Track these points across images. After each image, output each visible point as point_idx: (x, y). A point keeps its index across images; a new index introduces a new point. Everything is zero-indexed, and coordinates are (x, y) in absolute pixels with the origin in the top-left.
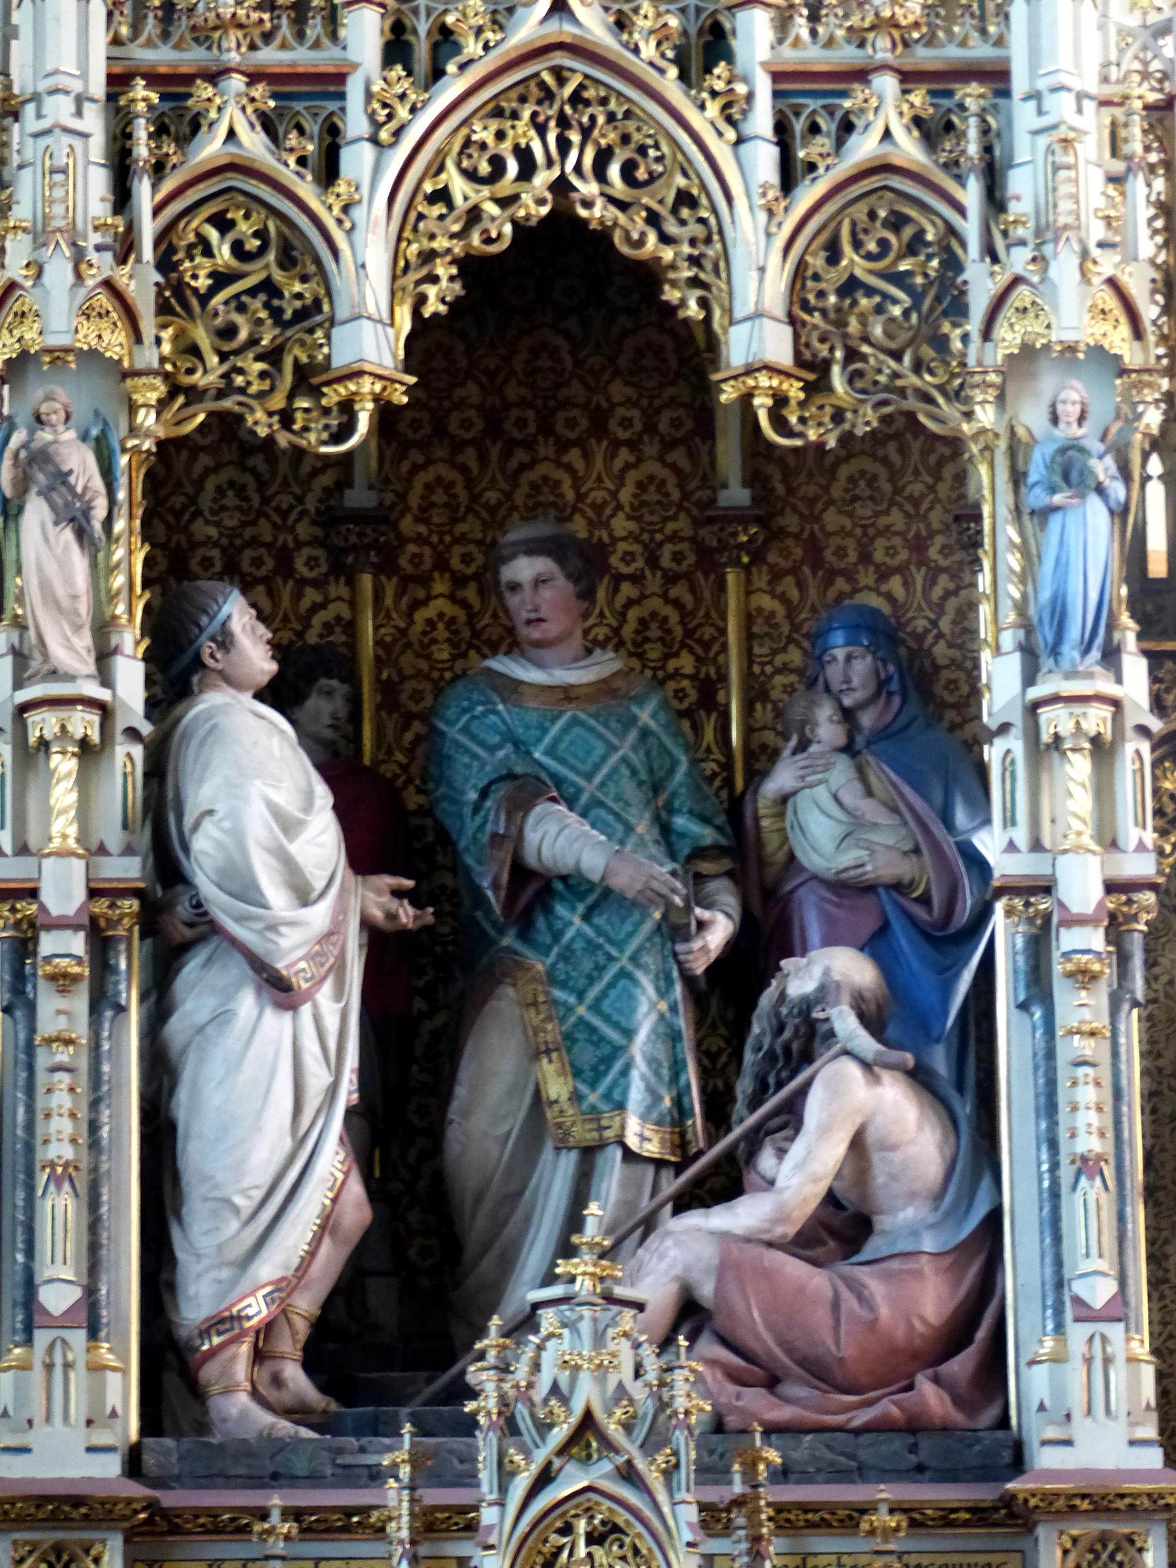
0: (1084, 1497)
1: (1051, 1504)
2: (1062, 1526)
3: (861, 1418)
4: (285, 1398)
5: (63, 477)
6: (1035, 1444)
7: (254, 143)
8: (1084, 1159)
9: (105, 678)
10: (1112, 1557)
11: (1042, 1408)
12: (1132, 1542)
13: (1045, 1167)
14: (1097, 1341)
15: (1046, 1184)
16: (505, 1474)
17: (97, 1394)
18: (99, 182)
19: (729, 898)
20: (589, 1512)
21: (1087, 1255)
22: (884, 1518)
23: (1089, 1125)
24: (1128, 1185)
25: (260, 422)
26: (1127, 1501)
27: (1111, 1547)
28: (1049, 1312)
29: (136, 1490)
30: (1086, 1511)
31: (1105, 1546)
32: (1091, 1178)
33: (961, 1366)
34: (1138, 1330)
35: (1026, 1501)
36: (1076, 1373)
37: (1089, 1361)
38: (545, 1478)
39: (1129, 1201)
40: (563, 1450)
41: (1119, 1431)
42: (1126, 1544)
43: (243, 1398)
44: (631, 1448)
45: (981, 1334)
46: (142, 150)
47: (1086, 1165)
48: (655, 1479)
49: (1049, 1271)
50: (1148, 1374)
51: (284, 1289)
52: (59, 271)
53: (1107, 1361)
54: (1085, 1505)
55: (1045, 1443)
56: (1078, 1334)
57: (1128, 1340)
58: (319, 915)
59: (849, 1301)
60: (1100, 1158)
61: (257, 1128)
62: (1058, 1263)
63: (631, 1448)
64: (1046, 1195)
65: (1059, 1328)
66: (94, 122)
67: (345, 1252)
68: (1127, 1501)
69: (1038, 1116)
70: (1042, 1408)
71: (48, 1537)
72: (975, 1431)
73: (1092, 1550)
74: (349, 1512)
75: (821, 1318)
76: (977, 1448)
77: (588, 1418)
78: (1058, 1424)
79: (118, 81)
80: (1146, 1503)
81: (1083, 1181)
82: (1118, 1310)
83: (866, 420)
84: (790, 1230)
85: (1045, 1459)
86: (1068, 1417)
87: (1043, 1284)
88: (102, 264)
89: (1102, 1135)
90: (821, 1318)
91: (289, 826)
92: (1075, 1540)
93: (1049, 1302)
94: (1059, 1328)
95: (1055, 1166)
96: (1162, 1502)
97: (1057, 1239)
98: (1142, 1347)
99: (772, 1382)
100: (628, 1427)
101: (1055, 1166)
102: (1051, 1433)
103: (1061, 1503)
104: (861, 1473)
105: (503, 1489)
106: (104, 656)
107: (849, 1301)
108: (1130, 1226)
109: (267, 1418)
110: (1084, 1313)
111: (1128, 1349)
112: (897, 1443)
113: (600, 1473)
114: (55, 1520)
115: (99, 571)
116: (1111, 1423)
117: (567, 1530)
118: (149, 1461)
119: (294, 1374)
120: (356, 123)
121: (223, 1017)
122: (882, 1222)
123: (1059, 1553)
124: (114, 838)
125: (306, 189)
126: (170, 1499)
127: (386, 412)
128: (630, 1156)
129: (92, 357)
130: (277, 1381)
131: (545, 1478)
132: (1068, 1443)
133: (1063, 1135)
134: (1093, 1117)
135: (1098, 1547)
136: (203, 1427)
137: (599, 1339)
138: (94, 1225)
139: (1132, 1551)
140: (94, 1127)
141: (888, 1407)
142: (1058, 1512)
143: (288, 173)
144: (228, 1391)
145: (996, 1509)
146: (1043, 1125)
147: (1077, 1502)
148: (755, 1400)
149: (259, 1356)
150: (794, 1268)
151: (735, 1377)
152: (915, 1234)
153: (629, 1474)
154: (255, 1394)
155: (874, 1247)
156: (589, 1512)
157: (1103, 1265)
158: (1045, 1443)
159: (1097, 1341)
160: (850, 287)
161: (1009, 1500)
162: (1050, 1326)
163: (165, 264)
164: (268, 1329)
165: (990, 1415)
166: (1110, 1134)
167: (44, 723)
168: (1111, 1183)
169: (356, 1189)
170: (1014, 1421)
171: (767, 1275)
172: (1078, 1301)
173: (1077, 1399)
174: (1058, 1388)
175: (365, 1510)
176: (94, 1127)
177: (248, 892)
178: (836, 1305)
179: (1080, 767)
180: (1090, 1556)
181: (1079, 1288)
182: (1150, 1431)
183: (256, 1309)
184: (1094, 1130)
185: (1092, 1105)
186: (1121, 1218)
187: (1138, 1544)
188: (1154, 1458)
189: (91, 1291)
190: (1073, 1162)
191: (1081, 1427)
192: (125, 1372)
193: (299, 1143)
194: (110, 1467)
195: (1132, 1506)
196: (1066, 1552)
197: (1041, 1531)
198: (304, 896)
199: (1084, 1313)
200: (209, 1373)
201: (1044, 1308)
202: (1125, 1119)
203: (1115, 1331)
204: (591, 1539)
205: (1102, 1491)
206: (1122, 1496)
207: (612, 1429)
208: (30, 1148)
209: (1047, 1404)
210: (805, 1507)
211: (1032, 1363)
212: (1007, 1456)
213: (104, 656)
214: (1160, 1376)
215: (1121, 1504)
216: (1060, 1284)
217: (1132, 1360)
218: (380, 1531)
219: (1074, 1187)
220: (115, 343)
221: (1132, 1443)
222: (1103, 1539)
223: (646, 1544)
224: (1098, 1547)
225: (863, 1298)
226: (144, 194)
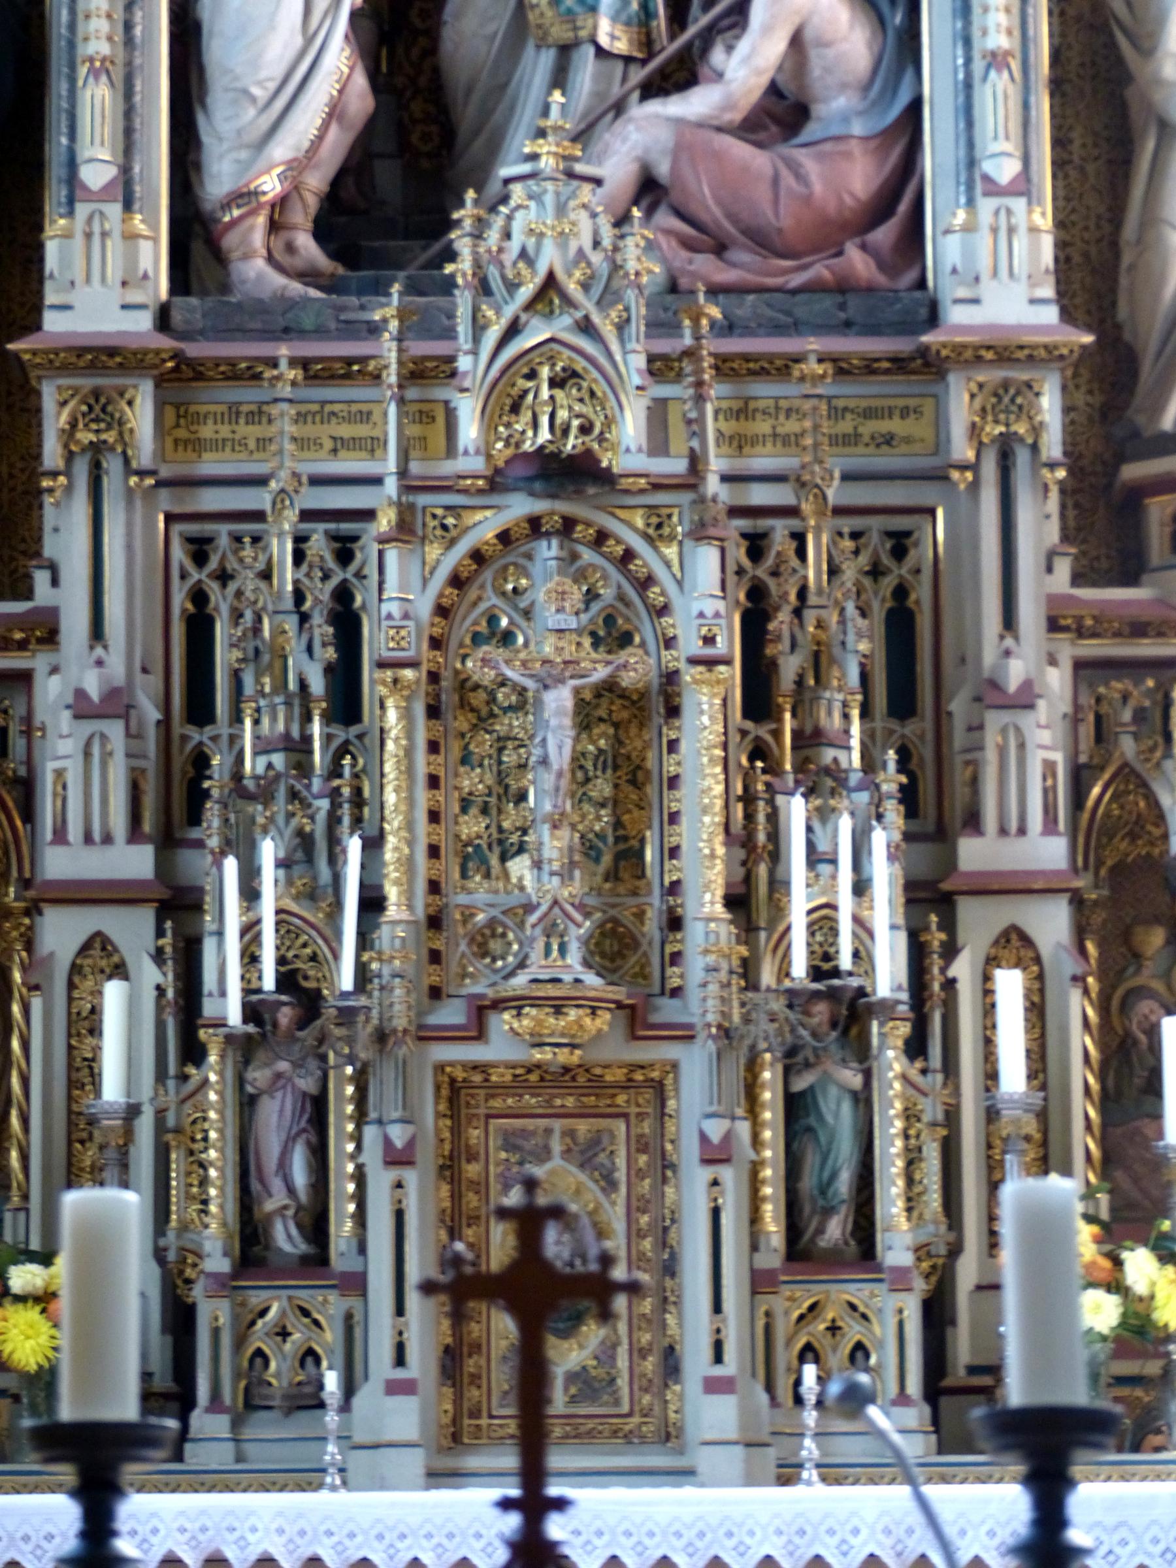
0: (989, 348)
1: (960, 354)
2: (971, 373)
3: (796, 280)
4: (298, 263)
6: (948, 303)
8: (994, 54)
10: (1013, 401)
11: (954, 271)
12: (1030, 387)
13: (960, 61)
14: (1003, 213)
15: (961, 76)
16: (479, 327)
17: (131, 259)
20: (552, 360)
21: (996, 138)
22: (813, 367)
23: (998, 25)
24: (1032, 76)
26: (1026, 352)
27: (1012, 391)
28: (962, 188)
29: (165, 342)
30: (991, 361)
31: (1006, 391)
32: (999, 71)
33: (884, 235)
34: (1040, 203)
35: (938, 352)
36: (984, 241)
37: (995, 230)
38: (513, 330)
39: (1033, 91)
40: (529, 306)
41: (1021, 290)
42: (1025, 389)
43: (259, 264)
44: (588, 305)
45: (903, 207)
47: (996, 60)
48: (608, 331)
49: (962, 153)
50: (1047, 245)
51: (296, 168)
53: (1011, 230)
54: (989, 355)
55: (957, 301)
56: (986, 206)
57: (1030, 212)
59: (788, 179)
60: (1008, 53)
61: (272, 27)
62: (970, 145)
63: (588, 305)
64: (960, 86)
65: (971, 202)
67: (349, 138)
68: (1026, 352)
69: (954, 17)
70: (954, 271)
71: (87, 383)
72: (896, 291)
73: (996, 395)
74: (349, 361)
75: (763, 194)
76: (898, 306)
77: (551, 280)
78: (968, 285)
80: (1043, 353)
81: (993, 74)
82: (1023, 186)
84: (737, 116)
85: (956, 315)
86: (977, 279)
87: (957, 164)
89: (1009, 32)
90: (763, 194)
92: (981, 386)
93: (963, 179)
94: (971, 202)
95: (968, 61)
96: (1056, 353)
97: (970, 124)
98: (1044, 218)
99: (720, 249)
100: (585, 286)
101: (968, 61)
102: (962, 293)
103: (968, 354)
104: (796, 327)
105: (476, 339)
107: (788, 179)
108: (1033, 113)
109: (278, 280)
110: (993, 189)
111: (1030, 220)
112: (827, 302)
113: (561, 325)
114: (93, 367)
116: (1013, 285)
117: (532, 375)
118: (177, 317)
119: (305, 242)
122: (819, 110)
123: (966, 397)
126: (194, 350)
128: (601, 52)
130: (290, 248)
131: (513, 330)
132: (976, 301)
133: (976, 33)
134: (1002, 18)
135: (1001, 391)
136: (225, 288)
137: (561, 210)
138: (129, 113)
139: (1030, 395)
140: (128, 26)
141: (820, 270)
142: (966, 361)
144: (247, 256)
145: (913, 359)
146: (959, 25)
147: (983, 353)
148: (705, 265)
149: (274, 227)
150: (740, 150)
151: (689, 245)
152: (846, 119)
153: (586, 327)
154: (270, 259)
155: (811, 131)
156: (552, 360)
157: (1008, 147)
158: (957, 301)
159: (1003, 213)
161: (923, 352)
162: (963, 200)
164: (282, 202)
165: (911, 276)
166: (1017, 33)
168: (1017, 75)
169: (360, 81)
170: (930, 283)
171: (718, 156)
172: (986, 178)
173: (984, 263)
174: (969, 253)
175: (363, 360)
176: (128, 26)
178: (776, 181)
180: (994, 400)
181: (987, 167)
182: (1048, 291)
183: (271, 185)
184: (1003, 29)
185: (1002, 8)
186: (1026, 106)
187: (1036, 389)
188: (1050, 315)
189: (126, 170)
190: (984, 57)
191: (987, 288)
192: (155, 240)
193: (309, 40)
194: (143, 322)
195: (1030, 357)
196: (973, 396)
197: (952, 378)
199: (993, 189)
200: (230, 241)
201: (958, 183)
202: (1031, 20)
203: (1019, 205)
204: (554, 383)
205: (1005, 343)
206: (1021, 347)
207: (572, 287)
208: (72, 45)
209: (959, 268)
210: (746, 358)
211: (947, 232)
212: (924, 312)
214: (1061, 246)
215: (1021, 355)
216: (972, 163)
217: (1033, 230)
218: (377, 377)
219: (985, 78)
221: (1033, 301)
222: (1006, 385)
223: (601, 388)
224: (1001, 391)
225: (799, 175)
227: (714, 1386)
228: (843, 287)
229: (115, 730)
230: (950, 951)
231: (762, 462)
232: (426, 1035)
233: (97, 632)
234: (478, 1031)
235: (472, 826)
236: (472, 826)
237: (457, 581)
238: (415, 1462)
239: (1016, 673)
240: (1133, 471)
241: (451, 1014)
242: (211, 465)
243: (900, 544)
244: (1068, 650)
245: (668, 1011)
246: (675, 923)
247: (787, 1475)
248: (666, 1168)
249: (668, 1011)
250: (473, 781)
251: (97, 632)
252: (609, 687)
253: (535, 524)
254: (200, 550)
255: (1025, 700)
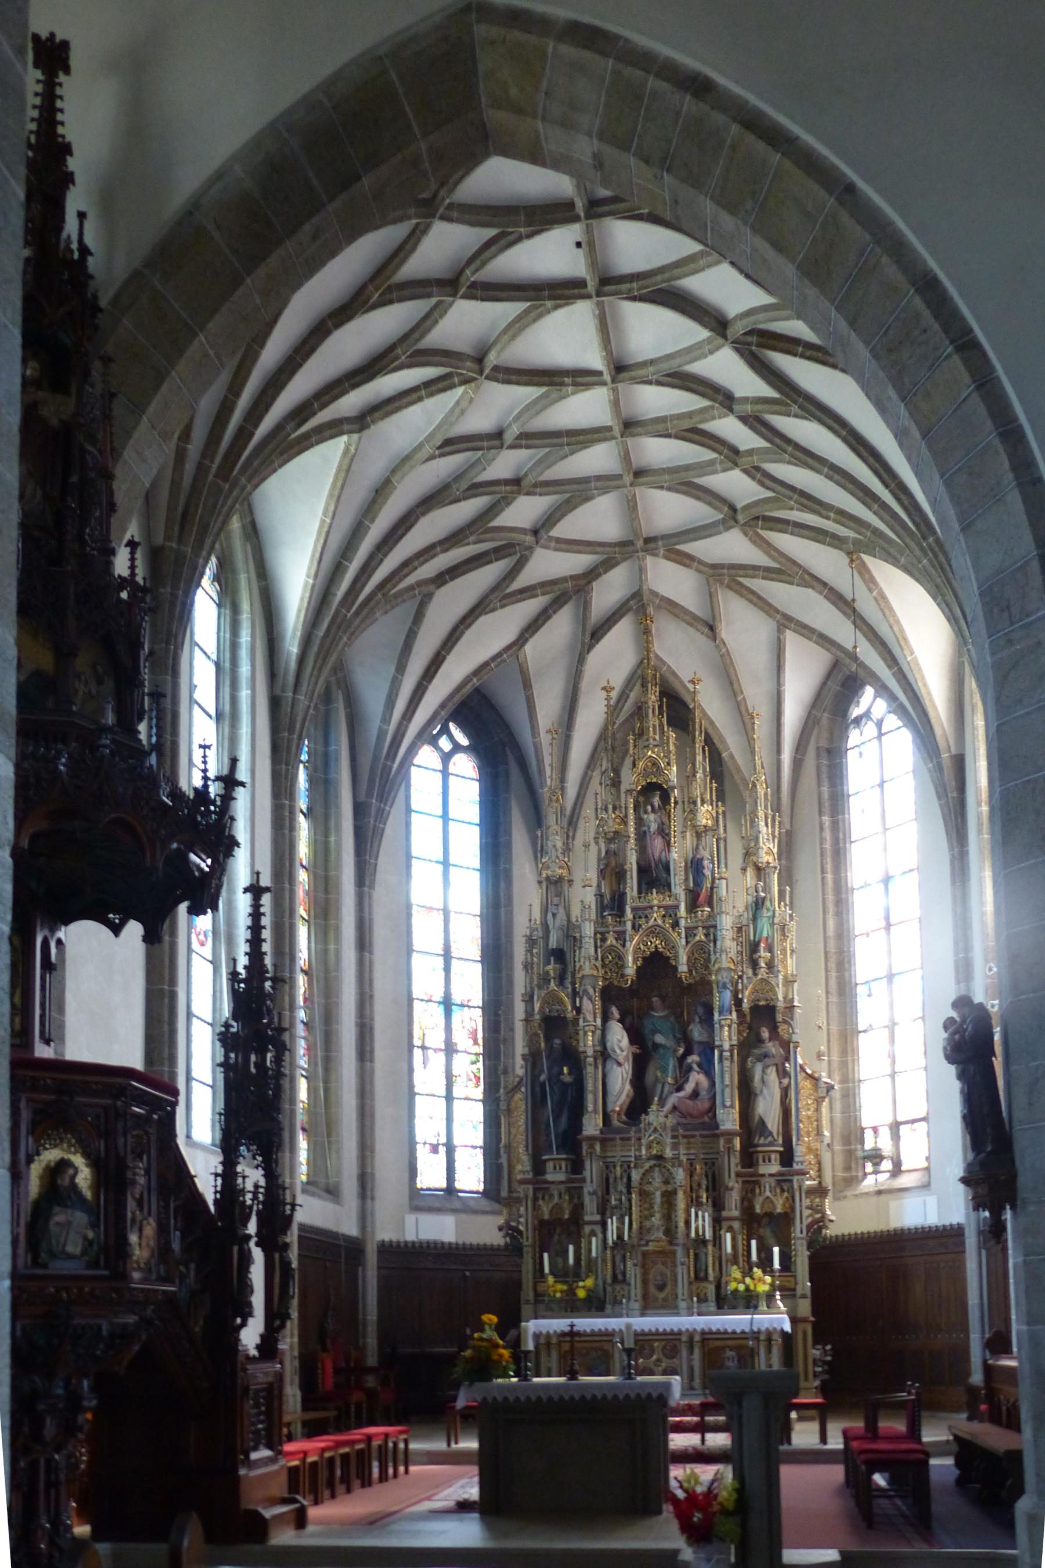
5: (588, 993)
7: (614, 942)
9: (595, 1021)
18: (593, 949)
19: (683, 1045)
25: (616, 983)
33: (710, 1114)
46: (599, 944)
51: (621, 1107)
52: (587, 963)
58: (625, 1053)
66: (592, 941)
79: (595, 934)
83: (697, 979)
85: (722, 1128)
88: (593, 962)
91: (620, 1041)
106: (595, 1017)
115: (594, 1005)
120: (628, 938)
121: (612, 1068)
124: (596, 1043)
125: (621, 948)
127: (632, 981)
129: (592, 975)
141: (700, 1121)
143: (618, 946)
148: (683, 1121)
160: (696, 959)
163: (602, 960)
167: (587, 1028)
177: (614, 1051)
179: (726, 1028)
183: (617, 1109)
198: (622, 1051)
213: (595, 1017)
220: (595, 973)
226: (599, 950)
227: (683, 1300)
228: (704, 1123)
229: (594, 1197)
230: (720, 1229)
231: (693, 1151)
232: (640, 1246)
233: (592, 1181)
234: (647, 1245)
235: (646, 1213)
236: (646, 1213)
237: (644, 1174)
238: (637, 1312)
239: (730, 1184)
240: (751, 1150)
241: (643, 1242)
242: (609, 1154)
243: (713, 1164)
244: (740, 1180)
245: (676, 1241)
246: (676, 1227)
247: (692, 1315)
248: (675, 1266)
249: (676, 1241)
250: (646, 1206)
251: (592, 1181)
252: (666, 1191)
253: (655, 1165)
254: (607, 1167)
255: (732, 1189)
